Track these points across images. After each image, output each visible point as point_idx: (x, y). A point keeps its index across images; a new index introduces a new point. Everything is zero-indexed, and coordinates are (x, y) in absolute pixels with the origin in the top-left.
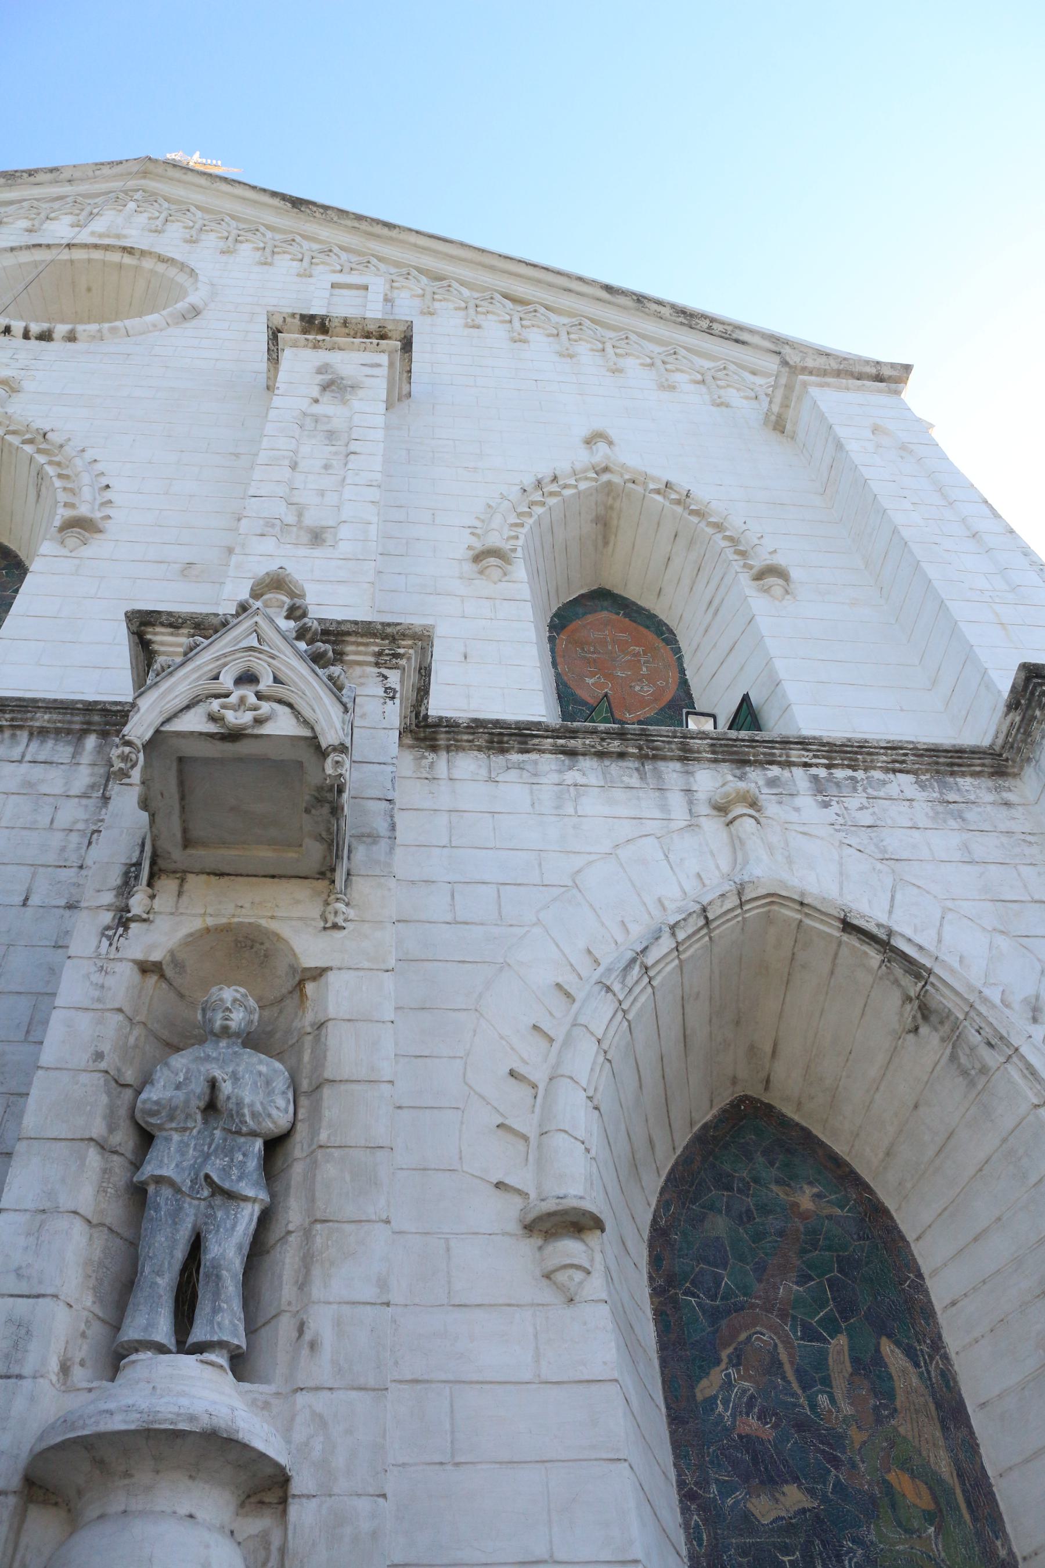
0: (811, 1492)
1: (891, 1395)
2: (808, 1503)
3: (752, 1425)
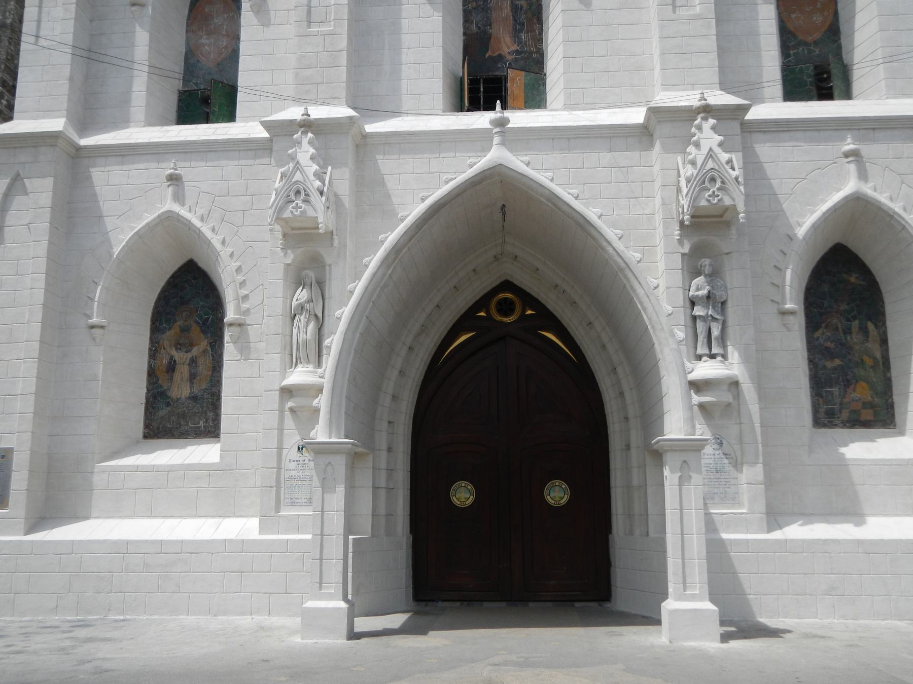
0: (842, 361)
1: (868, 337)
2: (840, 363)
3: (829, 344)
